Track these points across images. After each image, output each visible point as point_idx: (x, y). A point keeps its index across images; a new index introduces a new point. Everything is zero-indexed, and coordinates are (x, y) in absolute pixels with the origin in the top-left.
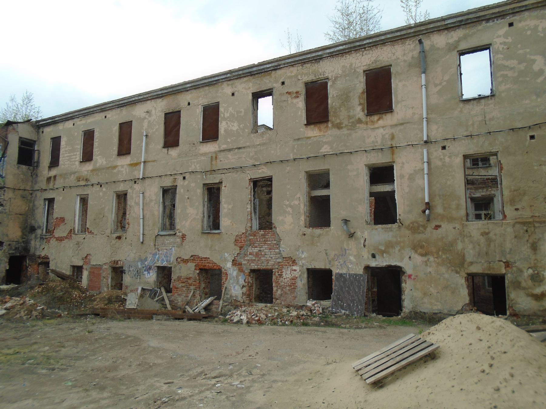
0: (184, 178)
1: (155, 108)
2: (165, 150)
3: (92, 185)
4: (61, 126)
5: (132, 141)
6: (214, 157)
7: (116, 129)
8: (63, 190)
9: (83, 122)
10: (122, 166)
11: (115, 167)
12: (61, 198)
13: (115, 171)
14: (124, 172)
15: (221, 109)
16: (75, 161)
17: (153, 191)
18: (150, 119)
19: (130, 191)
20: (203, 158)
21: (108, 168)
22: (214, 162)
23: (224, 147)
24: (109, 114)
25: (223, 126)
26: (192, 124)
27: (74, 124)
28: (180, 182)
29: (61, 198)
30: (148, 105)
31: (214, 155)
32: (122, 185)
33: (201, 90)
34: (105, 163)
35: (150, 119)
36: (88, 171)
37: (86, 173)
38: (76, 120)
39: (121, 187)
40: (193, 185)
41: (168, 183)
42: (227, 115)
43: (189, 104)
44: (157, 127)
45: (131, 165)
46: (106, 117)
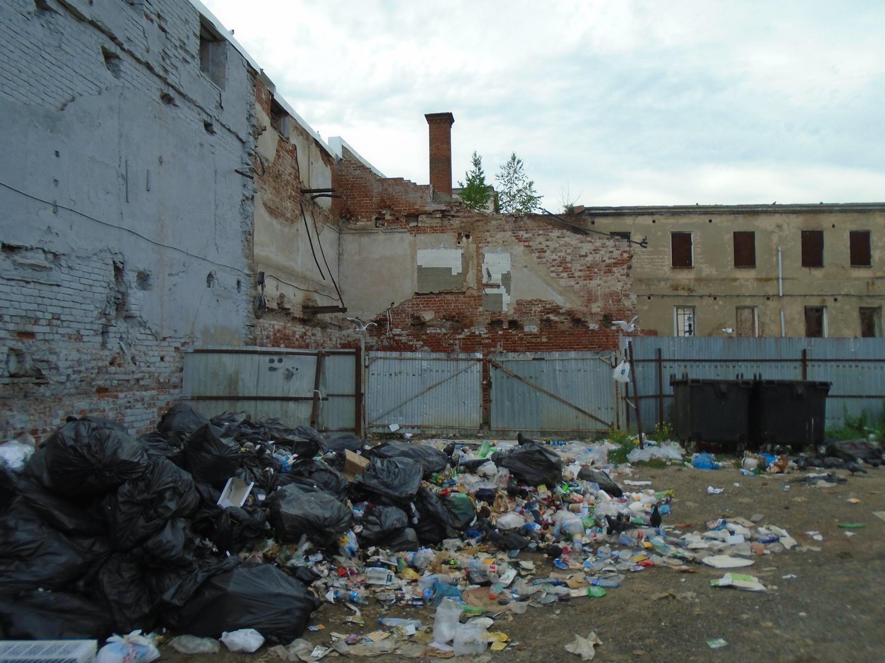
0: (836, 300)
1: (788, 224)
2: (806, 270)
3: (702, 297)
4: (629, 221)
5: (757, 254)
6: (871, 283)
7: (729, 238)
8: (649, 298)
9: (672, 220)
10: (747, 280)
11: (735, 280)
12: (646, 308)
13: (737, 283)
14: (750, 286)
15: (874, 238)
16: (662, 266)
17: (795, 311)
18: (781, 233)
19: (760, 307)
20: (857, 282)
21: (723, 280)
22: (871, 288)
23: (879, 274)
24: (716, 220)
25: (876, 255)
26: (836, 247)
27: (654, 222)
28: (830, 302)
29: (646, 308)
30: (778, 219)
31: (870, 281)
32: (749, 299)
33: (849, 215)
34: (715, 273)
35: (781, 233)
36: (690, 280)
37: (687, 282)
38: (656, 217)
39: (748, 302)
40: (847, 307)
41: (815, 302)
42: (881, 244)
43: (833, 226)
44: (793, 243)
45: (760, 280)
46: (710, 221)
